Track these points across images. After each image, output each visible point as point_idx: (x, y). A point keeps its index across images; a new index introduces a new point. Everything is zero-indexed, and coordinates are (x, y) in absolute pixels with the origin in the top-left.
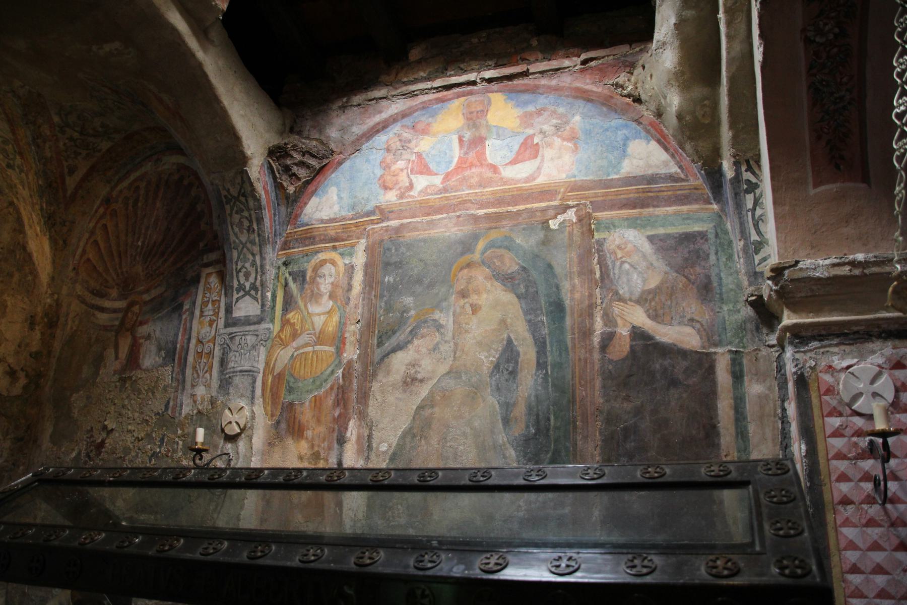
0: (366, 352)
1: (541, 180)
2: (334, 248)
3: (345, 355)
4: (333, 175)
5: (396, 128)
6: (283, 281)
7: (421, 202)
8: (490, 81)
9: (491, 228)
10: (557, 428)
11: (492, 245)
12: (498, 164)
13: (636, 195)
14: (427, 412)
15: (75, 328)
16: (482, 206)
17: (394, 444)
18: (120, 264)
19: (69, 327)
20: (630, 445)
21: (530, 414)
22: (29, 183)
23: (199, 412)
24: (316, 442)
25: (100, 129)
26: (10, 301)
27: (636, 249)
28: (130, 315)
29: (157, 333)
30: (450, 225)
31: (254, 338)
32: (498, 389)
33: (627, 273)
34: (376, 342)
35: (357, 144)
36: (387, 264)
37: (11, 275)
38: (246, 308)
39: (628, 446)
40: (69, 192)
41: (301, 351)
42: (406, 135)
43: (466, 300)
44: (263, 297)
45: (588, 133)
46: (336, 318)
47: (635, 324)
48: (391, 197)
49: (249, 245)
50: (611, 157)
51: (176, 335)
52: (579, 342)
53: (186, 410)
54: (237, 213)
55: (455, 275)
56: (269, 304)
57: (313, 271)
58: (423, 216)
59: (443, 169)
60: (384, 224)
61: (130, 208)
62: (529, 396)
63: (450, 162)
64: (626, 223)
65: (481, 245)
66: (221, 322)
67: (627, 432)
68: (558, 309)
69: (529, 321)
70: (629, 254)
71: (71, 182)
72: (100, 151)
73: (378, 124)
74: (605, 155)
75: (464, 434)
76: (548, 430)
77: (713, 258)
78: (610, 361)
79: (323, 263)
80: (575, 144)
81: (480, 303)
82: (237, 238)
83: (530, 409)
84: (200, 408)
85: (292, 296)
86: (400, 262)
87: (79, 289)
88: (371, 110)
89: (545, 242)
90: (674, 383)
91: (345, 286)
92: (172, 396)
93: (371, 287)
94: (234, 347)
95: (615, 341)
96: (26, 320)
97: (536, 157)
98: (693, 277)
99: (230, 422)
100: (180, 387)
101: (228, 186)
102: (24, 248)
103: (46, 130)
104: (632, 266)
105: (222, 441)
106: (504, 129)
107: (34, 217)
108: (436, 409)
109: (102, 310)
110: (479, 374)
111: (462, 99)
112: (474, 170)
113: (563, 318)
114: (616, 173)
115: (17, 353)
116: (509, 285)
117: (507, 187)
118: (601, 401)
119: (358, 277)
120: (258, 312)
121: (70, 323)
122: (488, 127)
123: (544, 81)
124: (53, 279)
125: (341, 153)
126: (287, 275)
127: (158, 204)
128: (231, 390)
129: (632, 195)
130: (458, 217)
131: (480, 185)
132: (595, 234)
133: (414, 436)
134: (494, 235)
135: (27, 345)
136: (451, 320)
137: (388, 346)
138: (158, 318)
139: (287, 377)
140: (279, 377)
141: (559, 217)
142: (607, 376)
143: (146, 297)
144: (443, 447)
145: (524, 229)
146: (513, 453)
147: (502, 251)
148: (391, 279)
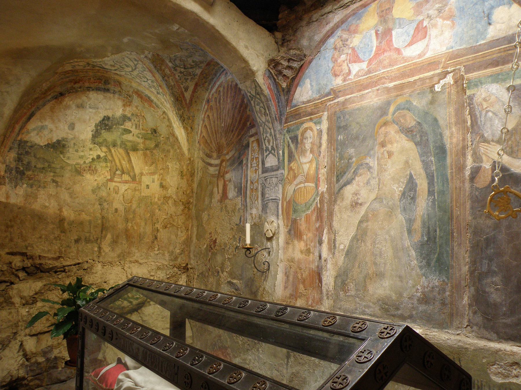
0: (330, 187)
1: (429, 55)
2: (311, 119)
3: (320, 188)
4: (307, 71)
5: (339, 33)
7: (356, 82)
9: (397, 96)
10: (441, 237)
11: (398, 108)
13: (499, 55)
14: (364, 225)
16: (392, 80)
17: (347, 245)
20: (490, 251)
21: (424, 227)
24: (308, 243)
25: (193, 64)
26: (170, 165)
27: (498, 99)
30: (373, 96)
32: (405, 209)
33: (491, 120)
36: (339, 128)
37: (168, 151)
38: (271, 161)
39: (488, 252)
40: (188, 102)
43: (385, 149)
44: (278, 154)
48: (338, 81)
49: (267, 123)
50: (479, 26)
51: (241, 179)
52: (456, 175)
55: (377, 132)
56: (281, 158)
57: (301, 135)
58: (357, 92)
59: (367, 57)
62: (424, 214)
63: (371, 51)
64: (490, 79)
65: (392, 109)
66: (260, 170)
67: (488, 242)
68: (441, 151)
69: (423, 161)
71: (188, 95)
72: (197, 74)
73: (328, 31)
74: (474, 25)
75: (386, 240)
76: (435, 238)
78: (477, 189)
79: (306, 129)
80: (452, 21)
81: (392, 150)
83: (424, 223)
85: (292, 153)
86: (346, 125)
88: (324, 22)
89: (432, 102)
91: (318, 144)
93: (331, 143)
94: (267, 186)
95: (481, 174)
96: (179, 174)
97: (425, 37)
101: (249, 90)
103: (167, 71)
104: (494, 113)
108: (369, 223)
110: (393, 199)
112: (386, 54)
113: (445, 158)
114: (483, 39)
116: (410, 136)
117: (407, 64)
118: (470, 218)
119: (325, 137)
120: (277, 163)
122: (394, 20)
124: (189, 150)
125: (310, 56)
126: (289, 139)
127: (229, 101)
129: (495, 56)
130: (378, 90)
131: (390, 65)
132: (467, 91)
133: (358, 240)
134: (400, 100)
135: (181, 188)
136: (376, 162)
137: (342, 182)
140: (289, 203)
141: (441, 81)
143: (228, 157)
144: (374, 247)
145: (418, 94)
146: (414, 253)
147: (406, 112)
148: (342, 137)
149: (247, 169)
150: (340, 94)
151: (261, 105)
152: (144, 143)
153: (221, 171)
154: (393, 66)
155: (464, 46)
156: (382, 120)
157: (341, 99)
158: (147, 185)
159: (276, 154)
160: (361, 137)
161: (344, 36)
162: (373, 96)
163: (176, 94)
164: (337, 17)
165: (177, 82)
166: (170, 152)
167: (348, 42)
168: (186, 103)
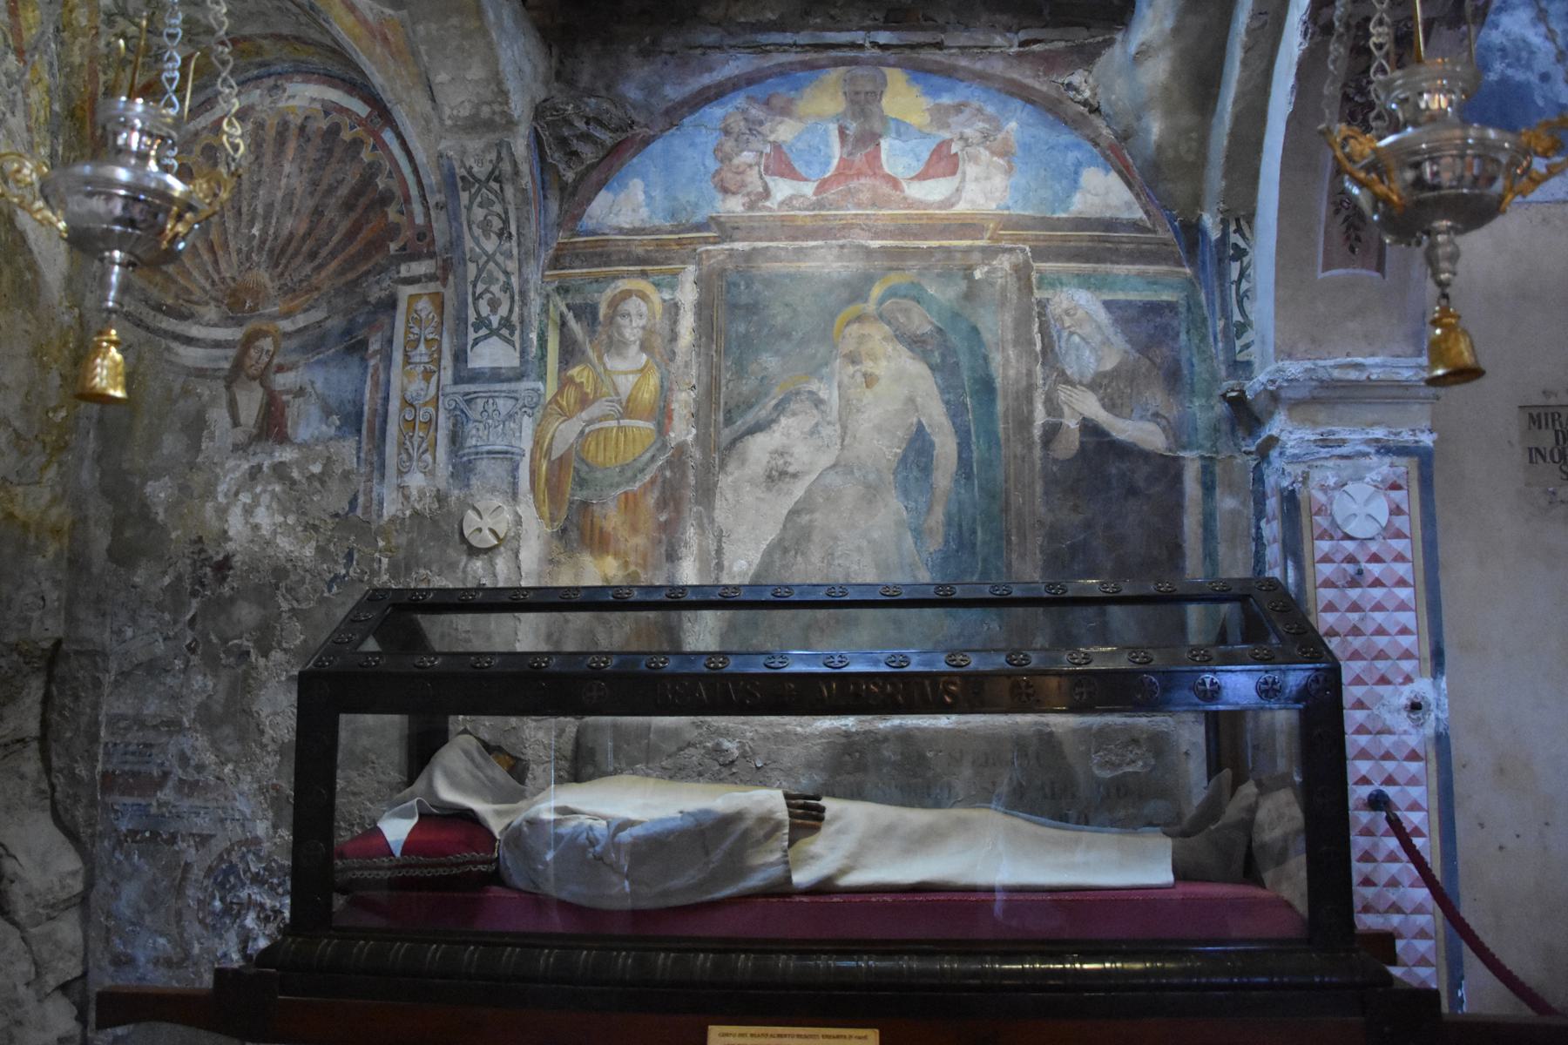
1: (961, 207)
2: (644, 274)
4: (635, 160)
5: (739, 100)
6: (558, 319)
7: (783, 219)
8: (884, 47)
9: (891, 269)
10: (984, 543)
11: (892, 293)
12: (899, 177)
14: (805, 519)
16: (877, 235)
18: (216, 262)
23: (416, 514)
28: (252, 352)
29: (319, 385)
31: (511, 403)
34: (721, 418)
35: (674, 115)
36: (733, 307)
41: (597, 426)
42: (756, 112)
44: (524, 340)
45: (1026, 148)
46: (653, 381)
47: (1087, 414)
48: (734, 206)
50: (1057, 187)
51: (359, 392)
53: (389, 510)
54: (481, 205)
57: (609, 306)
58: (787, 239)
60: (726, 246)
63: (828, 164)
65: (877, 291)
66: (447, 375)
68: (986, 387)
69: (947, 403)
70: (1080, 324)
75: (859, 549)
76: (974, 545)
77: (1183, 337)
78: (1055, 461)
79: (626, 295)
80: (1009, 162)
81: (877, 372)
82: (478, 244)
84: (418, 507)
85: (575, 342)
90: (1132, 491)
92: (361, 488)
97: (953, 173)
98: (1159, 361)
99: (480, 530)
100: (376, 474)
104: (1083, 339)
105: (464, 558)
106: (908, 126)
108: (817, 515)
109: (189, 341)
111: (842, 69)
112: (863, 181)
113: (993, 401)
114: (1066, 210)
115: (26, 409)
119: (687, 322)
120: (516, 363)
122: (884, 119)
123: (963, 62)
124: (69, 281)
126: (565, 309)
128: (474, 481)
130: (842, 247)
131: (874, 205)
133: (785, 551)
134: (895, 279)
136: (836, 393)
137: (739, 425)
139: (574, 464)
142: (1051, 481)
143: (287, 325)
144: (829, 564)
145: (939, 275)
149: (388, 368)
150: (737, 234)
151: (498, 208)
153: (248, 362)
154: (881, 208)
155: (1029, 212)
156: (852, 310)
157: (739, 246)
159: (516, 337)
160: (797, 336)
161: (753, 111)
162: (830, 258)
164: (735, 66)
167: (765, 128)
168: (93, 134)
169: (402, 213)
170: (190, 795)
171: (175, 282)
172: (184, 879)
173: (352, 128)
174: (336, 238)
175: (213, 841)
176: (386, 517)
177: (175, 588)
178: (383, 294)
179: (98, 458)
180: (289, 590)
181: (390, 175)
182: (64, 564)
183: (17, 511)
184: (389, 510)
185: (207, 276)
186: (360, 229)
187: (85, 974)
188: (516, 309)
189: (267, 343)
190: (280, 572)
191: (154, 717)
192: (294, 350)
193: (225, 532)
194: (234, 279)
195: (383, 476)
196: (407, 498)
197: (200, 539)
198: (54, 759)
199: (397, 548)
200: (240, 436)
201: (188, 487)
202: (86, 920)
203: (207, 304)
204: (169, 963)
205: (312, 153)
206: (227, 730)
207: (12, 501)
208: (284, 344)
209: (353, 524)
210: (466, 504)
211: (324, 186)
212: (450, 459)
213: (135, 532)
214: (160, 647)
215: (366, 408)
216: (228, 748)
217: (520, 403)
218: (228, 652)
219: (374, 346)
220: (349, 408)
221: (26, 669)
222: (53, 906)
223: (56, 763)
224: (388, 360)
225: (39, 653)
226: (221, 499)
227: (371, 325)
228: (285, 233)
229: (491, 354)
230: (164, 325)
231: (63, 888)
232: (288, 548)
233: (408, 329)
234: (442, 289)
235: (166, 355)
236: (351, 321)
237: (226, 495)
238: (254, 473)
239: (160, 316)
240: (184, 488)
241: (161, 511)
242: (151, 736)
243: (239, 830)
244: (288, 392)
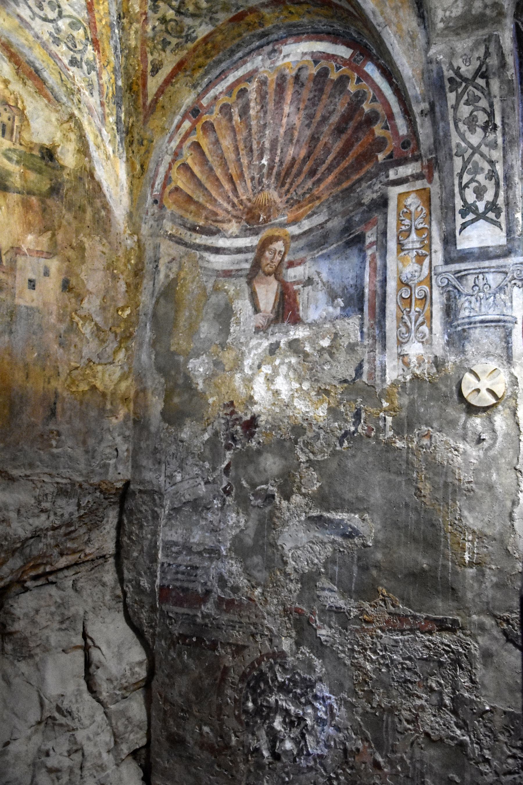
15: (172, 276)
18: (235, 190)
19: (162, 276)
22: (101, 85)
23: (415, 377)
28: (267, 254)
29: (325, 276)
31: (500, 277)
51: (360, 277)
53: (391, 375)
54: (467, 103)
61: (236, 118)
82: (464, 139)
84: (418, 372)
87: (169, 227)
92: (366, 357)
99: (478, 390)
100: (378, 346)
102: (92, 175)
107: (104, 132)
109: (217, 251)
115: (103, 308)
120: (503, 241)
121: (162, 268)
124: (130, 215)
128: (469, 347)
138: (322, 256)
143: (294, 230)
151: (483, 103)
152: (23, 176)
153: (264, 262)
158: (30, 281)
159: (502, 219)
163: (131, 68)
165: (144, 42)
166: (84, 211)
168: (144, 104)
169: (386, 128)
170: (227, 611)
171: (204, 208)
172: (223, 680)
173: (338, 68)
174: (330, 158)
175: (246, 651)
176: (388, 382)
177: (213, 442)
178: (375, 196)
179: (154, 344)
180: (306, 444)
181: (374, 100)
182: (130, 424)
183: (98, 384)
184: (391, 375)
185: (228, 200)
186: (352, 145)
187: (148, 746)
188: (502, 193)
189: (279, 246)
190: (298, 430)
191: (198, 545)
192: (302, 249)
193: (251, 397)
194: (249, 200)
195: (384, 347)
196: (407, 364)
197: (232, 403)
198: (125, 571)
199: (401, 407)
200: (260, 320)
201: (221, 362)
202: (148, 701)
203: (230, 221)
204: (211, 749)
205: (306, 94)
206: (257, 559)
207: (94, 377)
208: (293, 245)
209: (360, 388)
210: (463, 368)
211: (318, 118)
212: (445, 329)
213: (182, 400)
214: (202, 489)
215: (366, 291)
216: (257, 575)
217: (510, 276)
218: (256, 495)
219: (370, 238)
220: (352, 291)
221: (106, 502)
222: (125, 688)
223: (127, 575)
224: (384, 249)
225: (114, 491)
226: (247, 371)
227: (366, 221)
228: (288, 159)
229: (478, 236)
230: (198, 241)
231: (133, 674)
232: (304, 409)
233: (400, 222)
234: (428, 186)
235: (200, 262)
236: (349, 221)
237: (251, 368)
238: (273, 349)
239: (194, 235)
240: (217, 364)
241: (200, 381)
242: (196, 560)
243: (267, 643)
244: (298, 283)
